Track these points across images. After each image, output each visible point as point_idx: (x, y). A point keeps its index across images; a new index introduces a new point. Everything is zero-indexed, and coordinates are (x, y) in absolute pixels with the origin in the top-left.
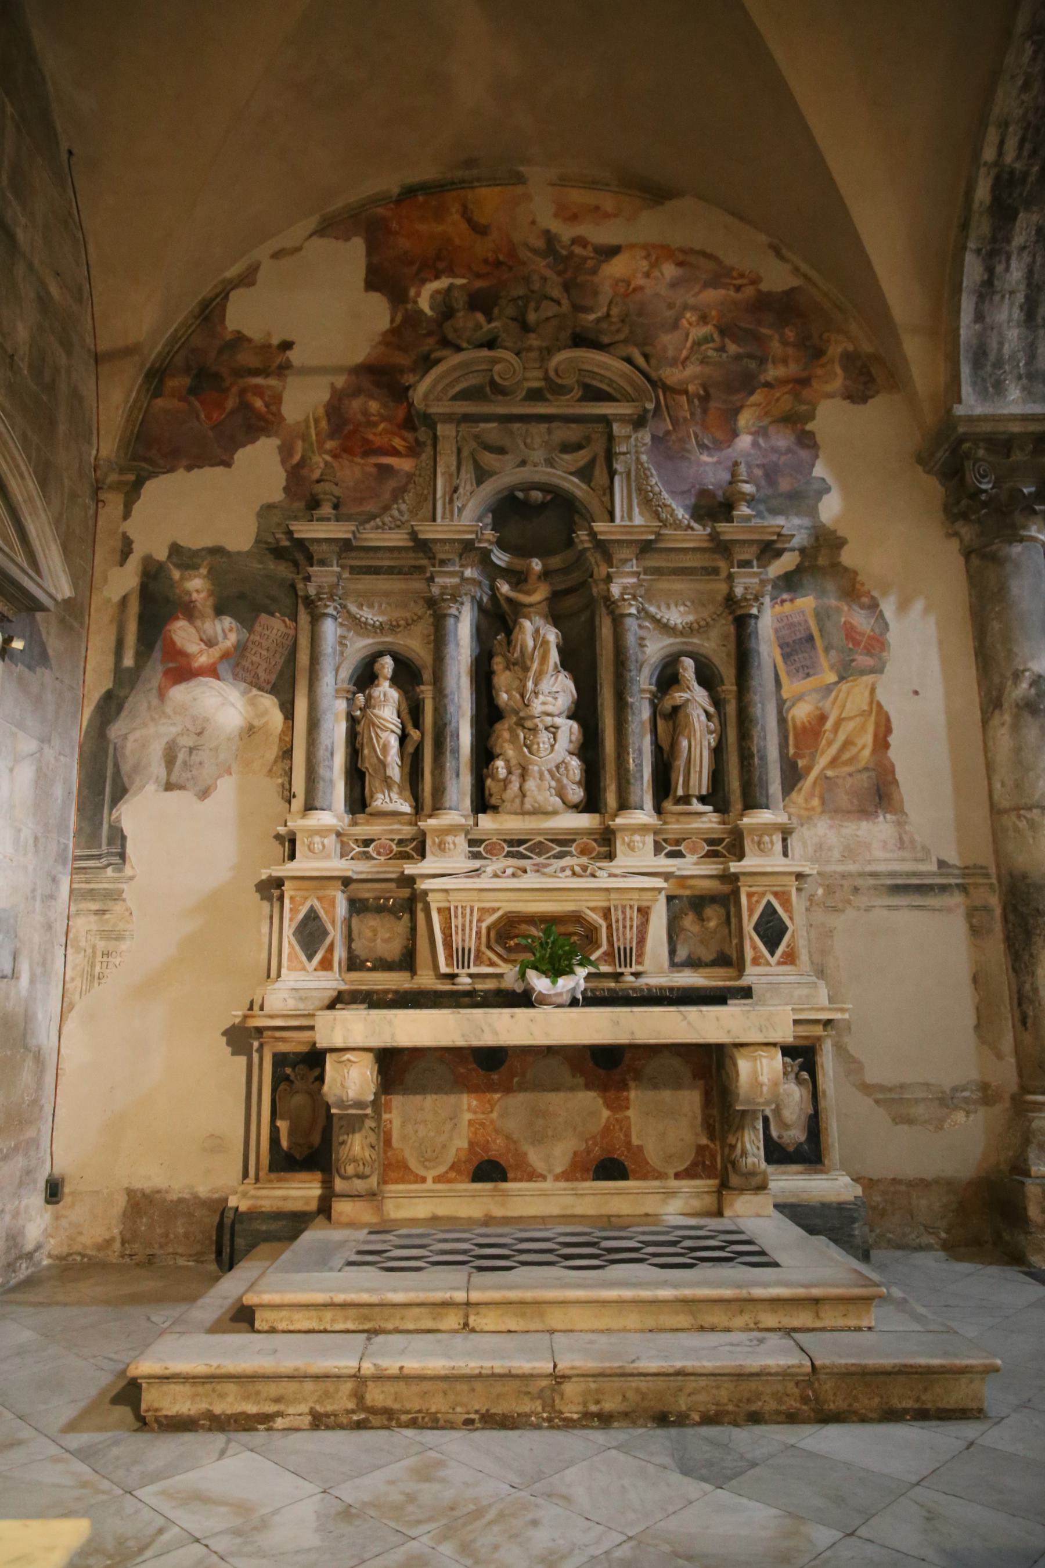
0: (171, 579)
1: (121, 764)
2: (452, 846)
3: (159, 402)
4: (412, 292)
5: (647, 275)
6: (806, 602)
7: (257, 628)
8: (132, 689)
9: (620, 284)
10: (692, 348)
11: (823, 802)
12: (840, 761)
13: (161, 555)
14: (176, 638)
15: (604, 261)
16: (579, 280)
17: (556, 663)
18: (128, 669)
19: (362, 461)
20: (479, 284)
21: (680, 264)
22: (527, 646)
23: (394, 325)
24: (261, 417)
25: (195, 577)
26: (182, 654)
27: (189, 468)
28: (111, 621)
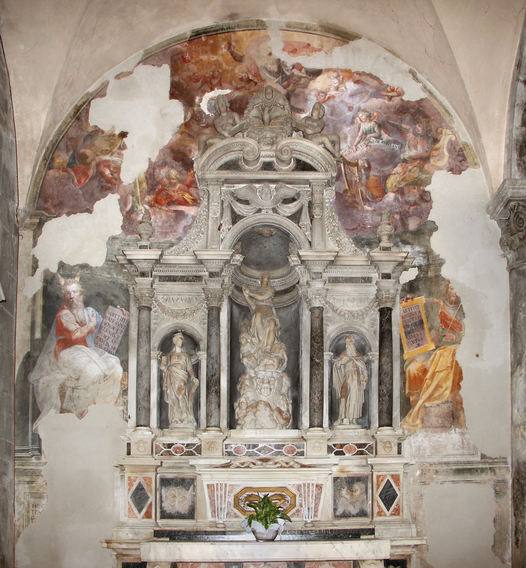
0: (60, 284)
1: (36, 396)
3: (51, 172)
4: (197, 99)
5: (337, 89)
6: (421, 300)
7: (108, 315)
8: (40, 352)
9: (321, 94)
10: (362, 136)
11: (423, 421)
12: (434, 397)
13: (54, 269)
14: (63, 321)
15: (311, 80)
16: (296, 92)
18: (38, 339)
19: (167, 209)
20: (237, 94)
21: (357, 82)
23: (186, 121)
24: (109, 181)
25: (72, 282)
26: (67, 330)
27: (69, 214)
28: (28, 310)
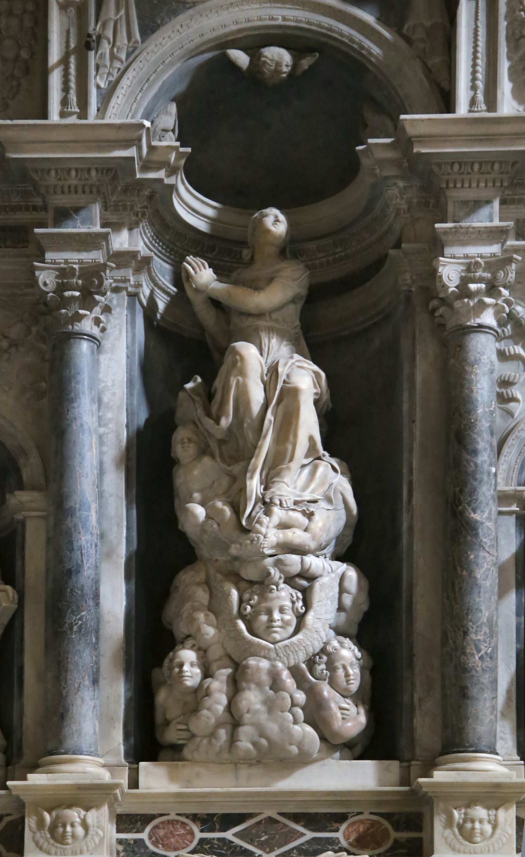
2: (80, 831)
17: (311, 439)
22: (248, 404)
